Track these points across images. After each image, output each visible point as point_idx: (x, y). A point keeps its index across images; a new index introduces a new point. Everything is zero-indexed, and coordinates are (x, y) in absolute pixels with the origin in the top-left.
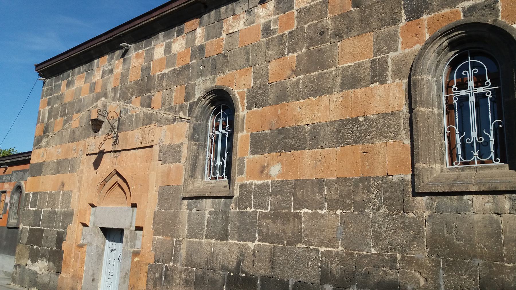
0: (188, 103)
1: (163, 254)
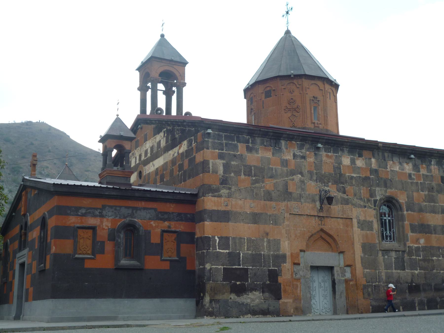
0: (373, 199)
1: (371, 279)
